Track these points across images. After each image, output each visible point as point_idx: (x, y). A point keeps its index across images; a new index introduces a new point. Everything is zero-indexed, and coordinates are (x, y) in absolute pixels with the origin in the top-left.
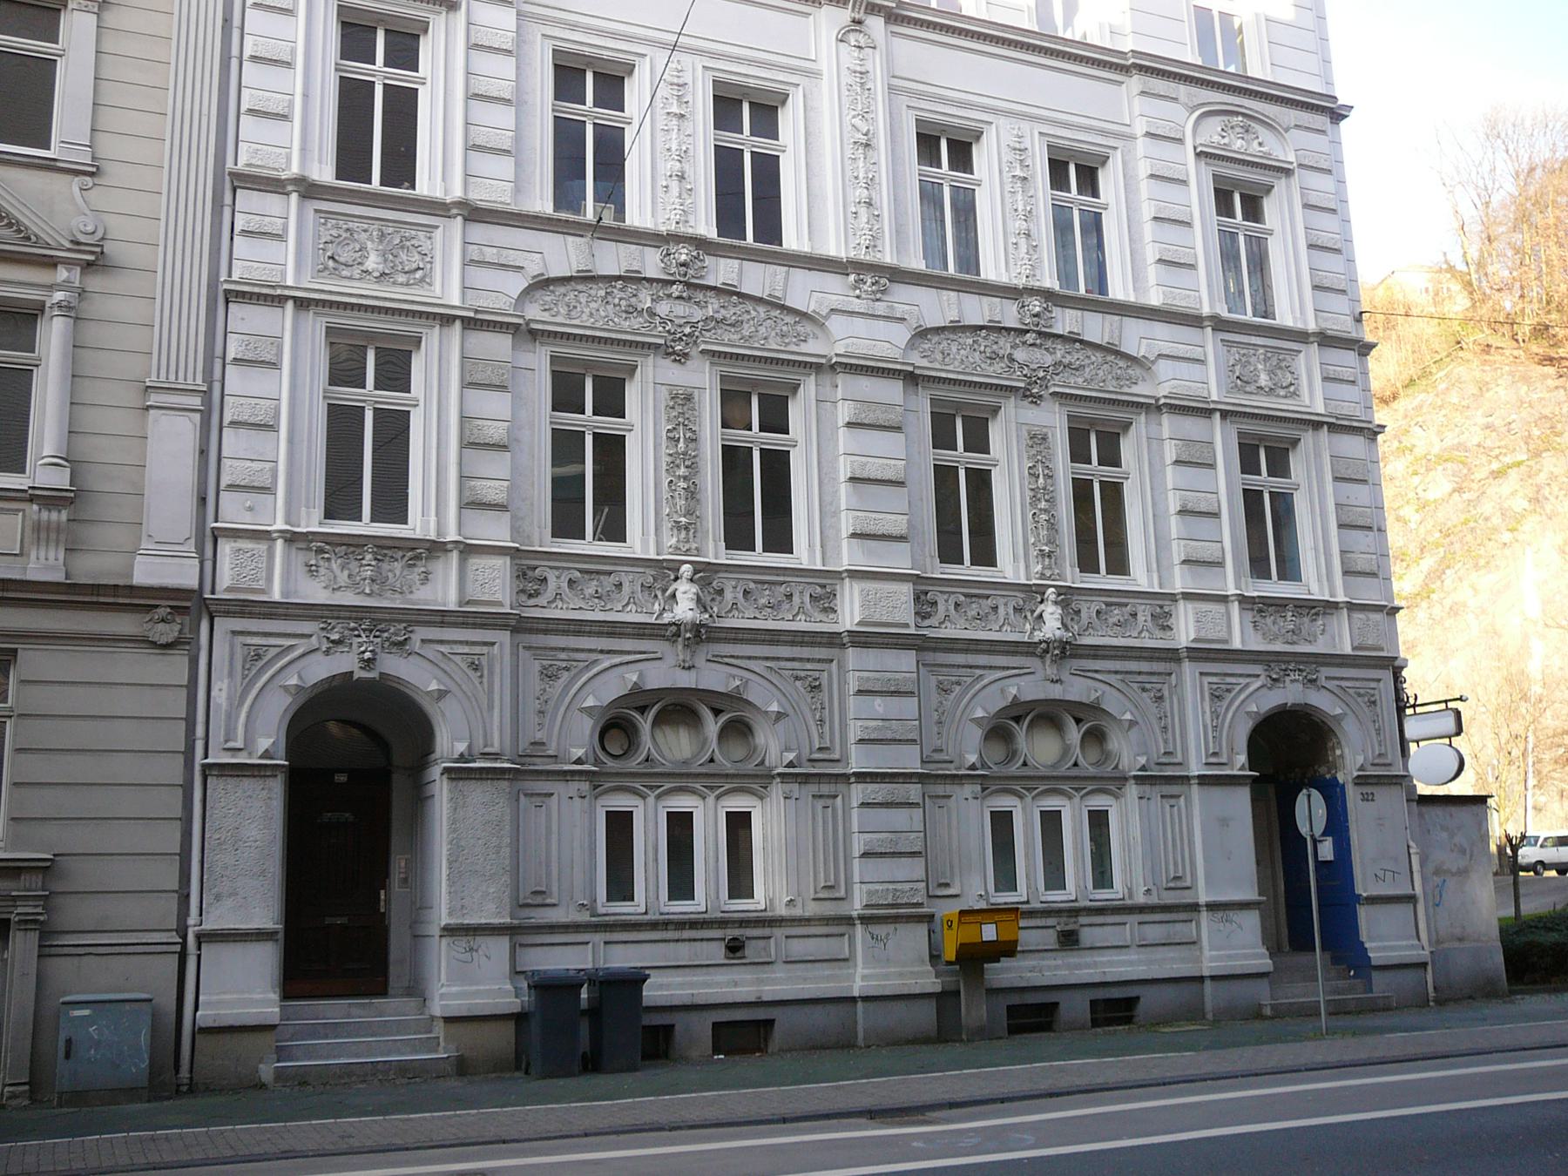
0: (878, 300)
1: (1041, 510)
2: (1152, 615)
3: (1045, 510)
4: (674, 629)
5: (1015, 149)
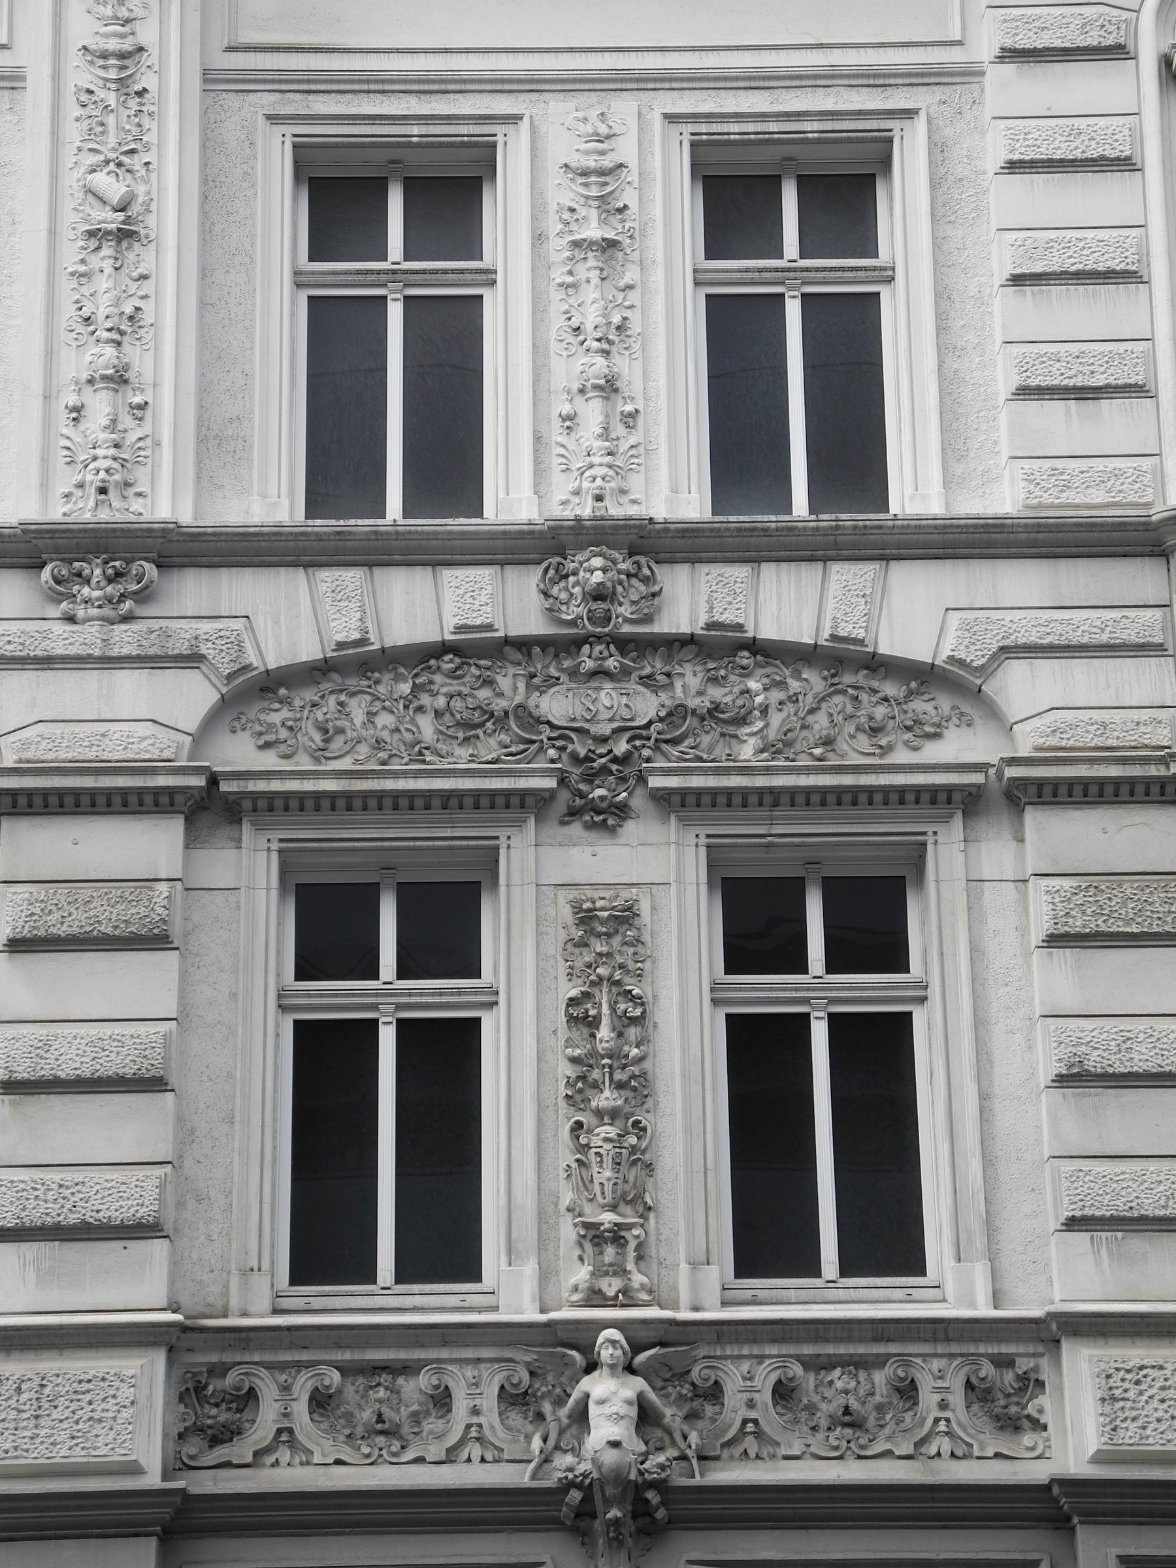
0: (127, 619)
1: (599, 1113)
2: (969, 1386)
3: (614, 1114)
4: (575, 1496)
5: (585, 173)
